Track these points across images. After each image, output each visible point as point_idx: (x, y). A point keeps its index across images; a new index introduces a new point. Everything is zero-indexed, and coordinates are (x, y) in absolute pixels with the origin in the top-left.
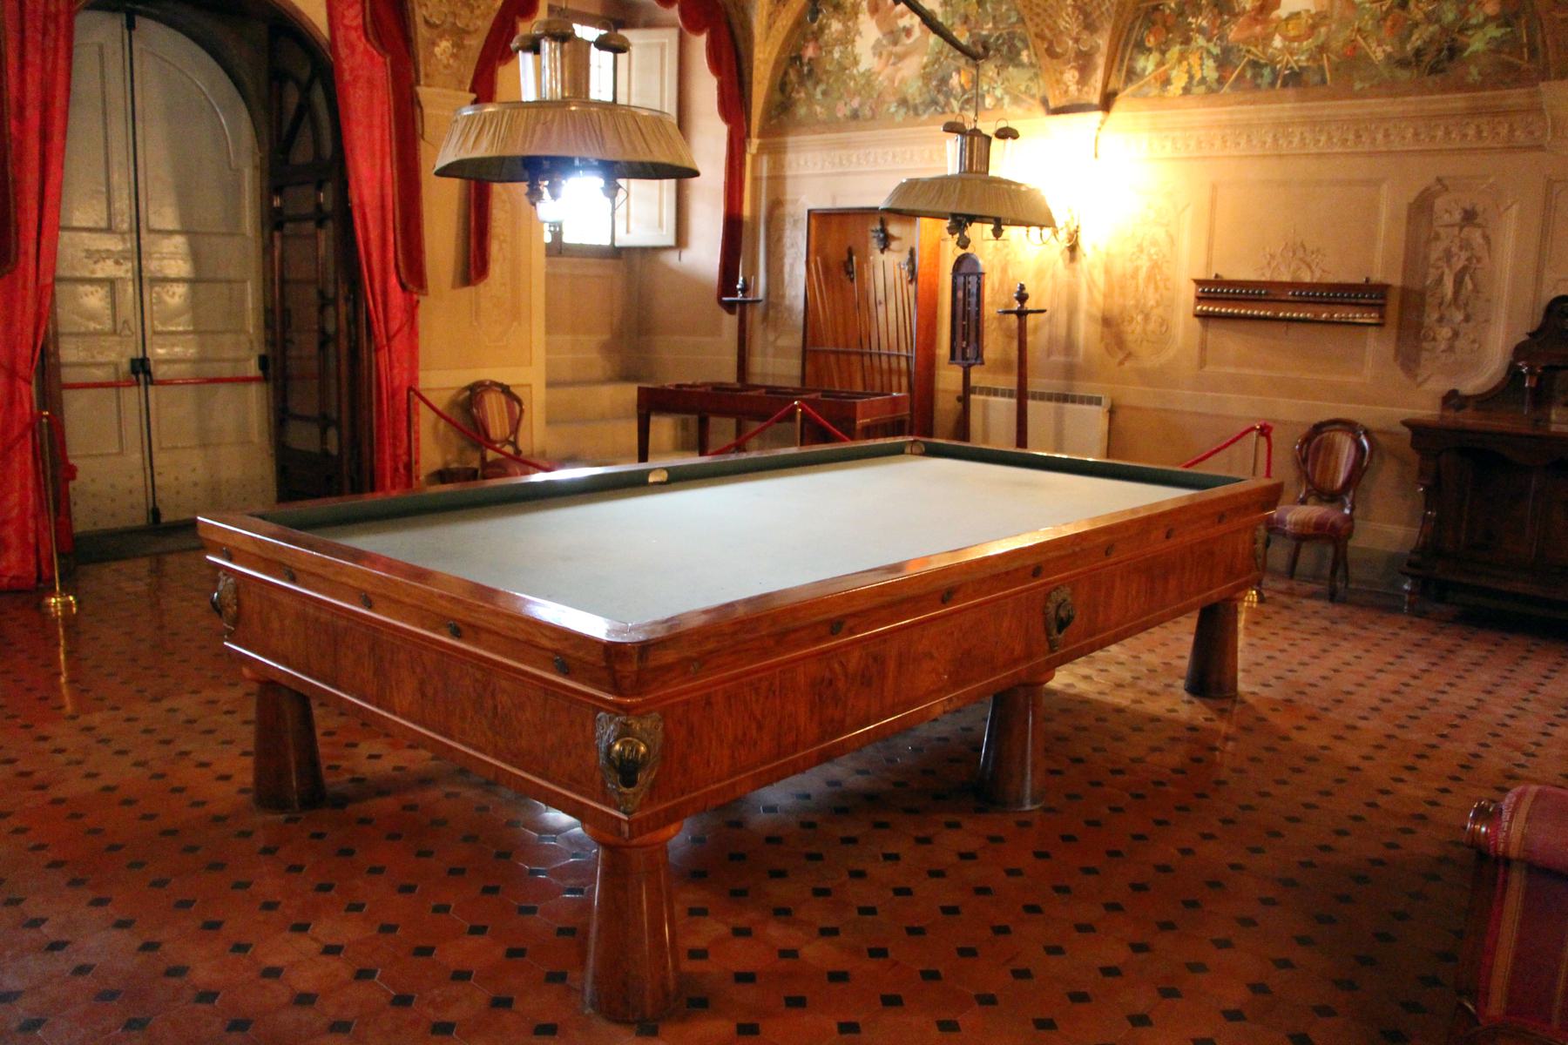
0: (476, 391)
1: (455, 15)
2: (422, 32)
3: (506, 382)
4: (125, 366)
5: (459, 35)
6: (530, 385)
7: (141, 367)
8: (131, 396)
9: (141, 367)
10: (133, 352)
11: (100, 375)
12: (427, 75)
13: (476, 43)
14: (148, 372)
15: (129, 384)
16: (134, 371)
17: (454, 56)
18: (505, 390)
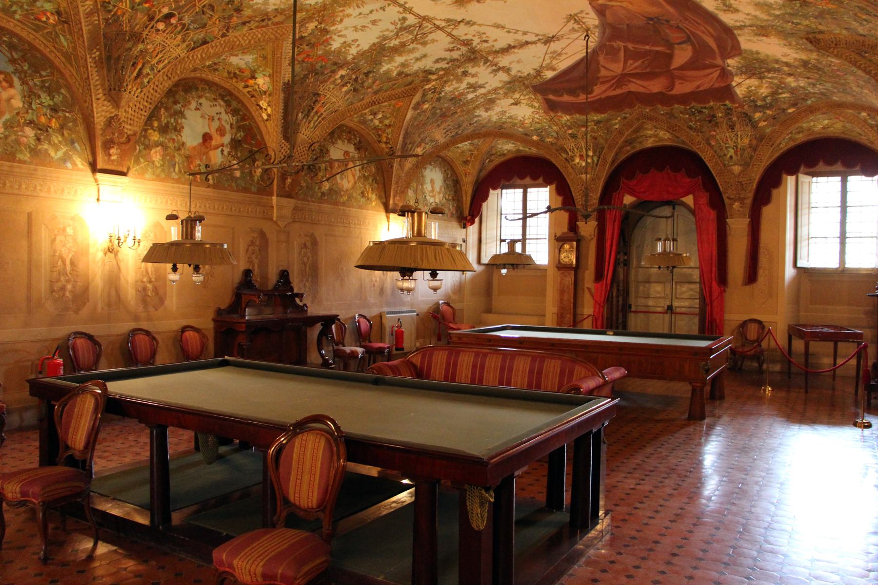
0: (744, 324)
1: (739, 194)
2: (727, 201)
3: (762, 320)
4: (666, 308)
5: (742, 200)
6: (776, 322)
7: (670, 308)
8: (667, 316)
9: (670, 308)
10: (668, 303)
11: (659, 309)
12: (731, 215)
13: (749, 202)
14: (672, 310)
15: (667, 313)
16: (668, 309)
17: (741, 207)
18: (759, 322)
